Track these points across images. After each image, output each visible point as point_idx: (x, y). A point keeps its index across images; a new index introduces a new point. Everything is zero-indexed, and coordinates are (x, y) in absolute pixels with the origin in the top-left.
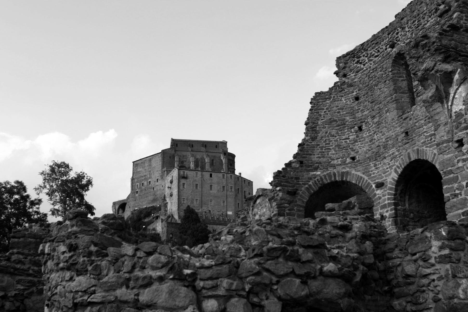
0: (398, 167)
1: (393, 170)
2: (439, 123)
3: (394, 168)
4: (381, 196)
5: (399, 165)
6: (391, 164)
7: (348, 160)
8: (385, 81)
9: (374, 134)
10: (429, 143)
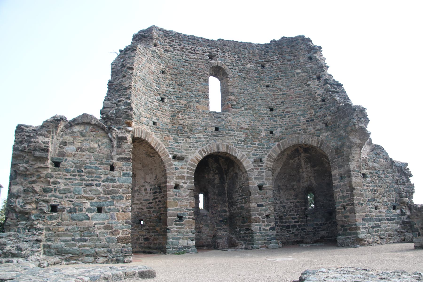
0: (203, 150)
1: (197, 151)
2: (353, 159)
3: (199, 149)
4: (179, 167)
5: (205, 150)
6: (196, 145)
7: (151, 123)
8: (200, 78)
9: (178, 112)
10: (239, 146)
